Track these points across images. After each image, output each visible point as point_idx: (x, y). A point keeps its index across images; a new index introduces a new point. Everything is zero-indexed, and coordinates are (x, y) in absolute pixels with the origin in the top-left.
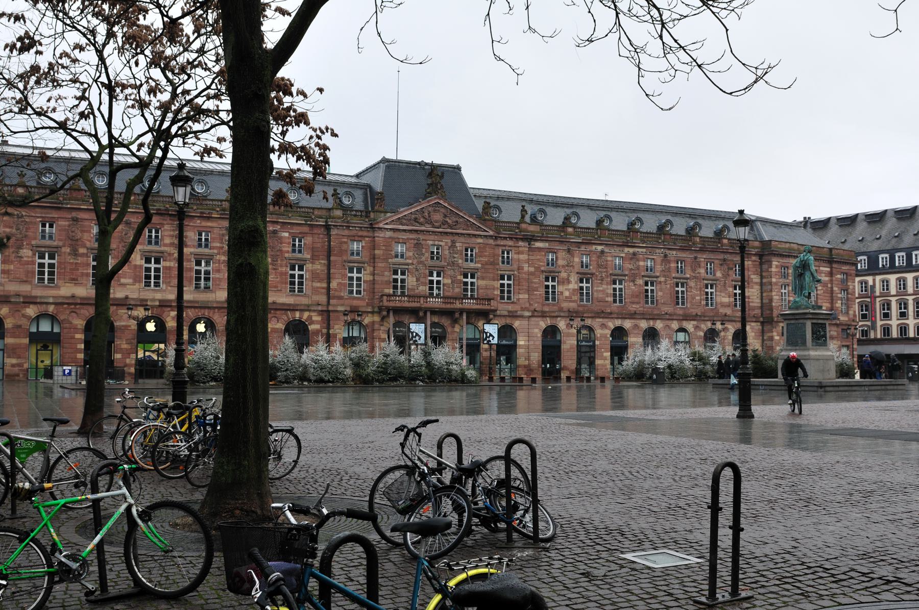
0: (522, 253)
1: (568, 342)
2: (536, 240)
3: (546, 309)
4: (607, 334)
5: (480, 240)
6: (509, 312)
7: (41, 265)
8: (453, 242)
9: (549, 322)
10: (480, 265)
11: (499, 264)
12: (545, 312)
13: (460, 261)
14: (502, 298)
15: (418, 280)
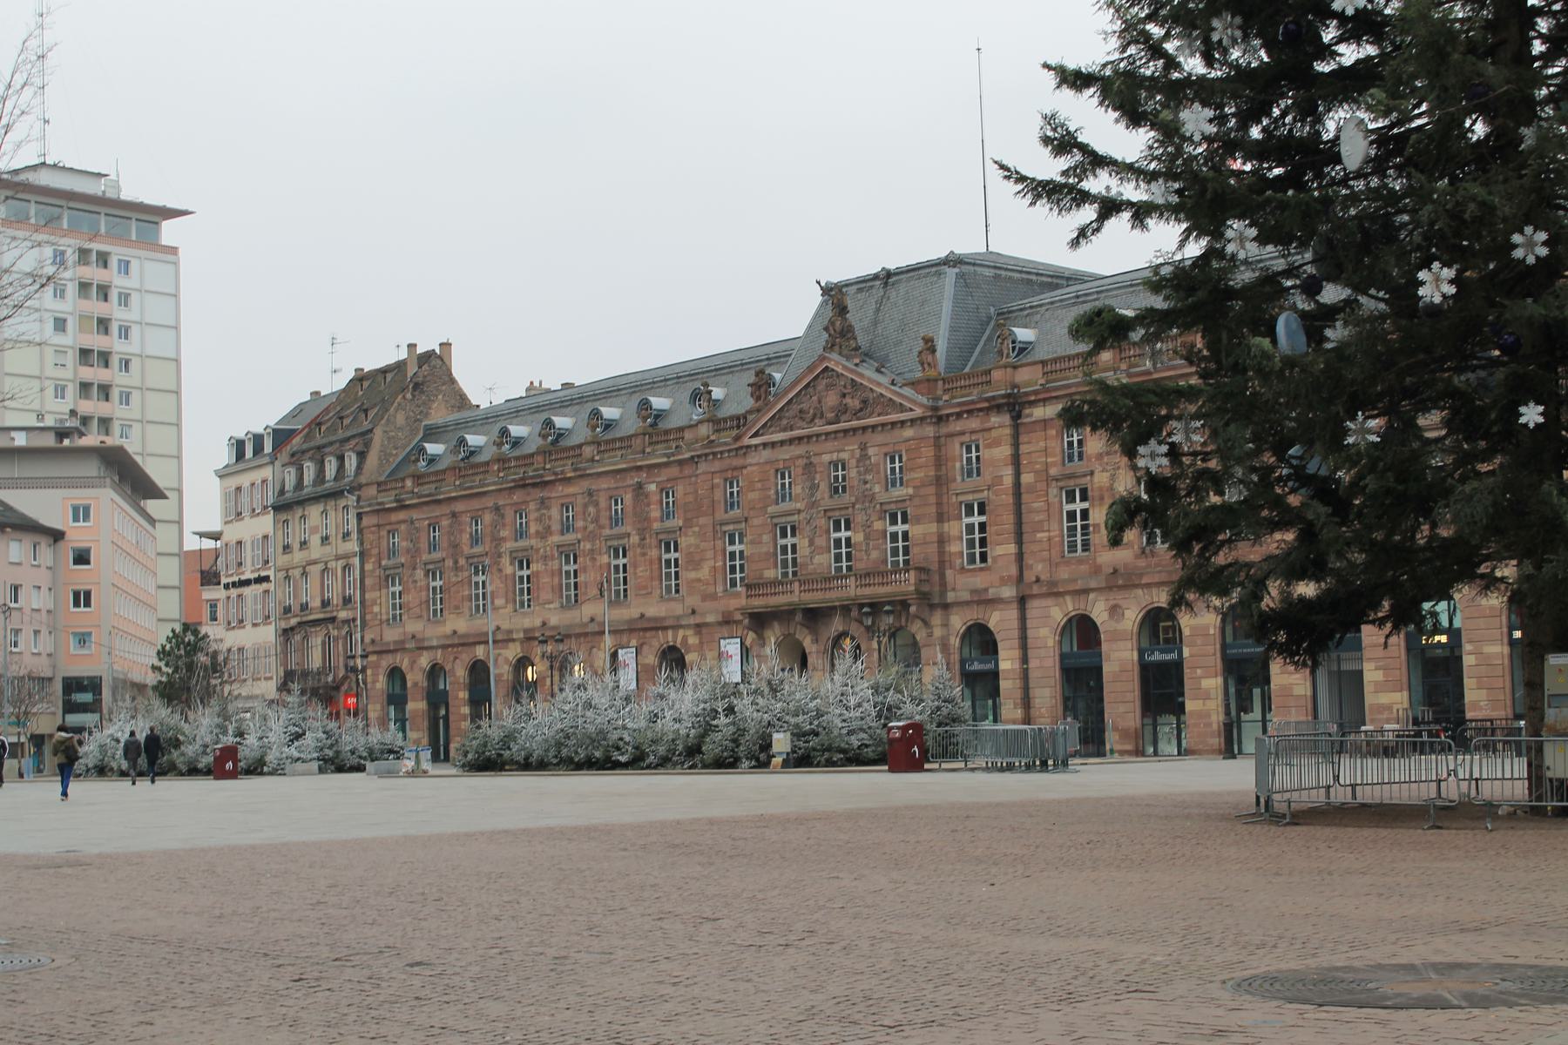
0: (996, 443)
1: (1114, 655)
2: (1032, 403)
3: (1064, 573)
4: (1207, 627)
5: (909, 433)
6: (974, 592)
8: (863, 447)
9: (1070, 606)
10: (911, 491)
11: (955, 480)
12: (1053, 584)
13: (877, 488)
14: (972, 560)
15: (811, 543)
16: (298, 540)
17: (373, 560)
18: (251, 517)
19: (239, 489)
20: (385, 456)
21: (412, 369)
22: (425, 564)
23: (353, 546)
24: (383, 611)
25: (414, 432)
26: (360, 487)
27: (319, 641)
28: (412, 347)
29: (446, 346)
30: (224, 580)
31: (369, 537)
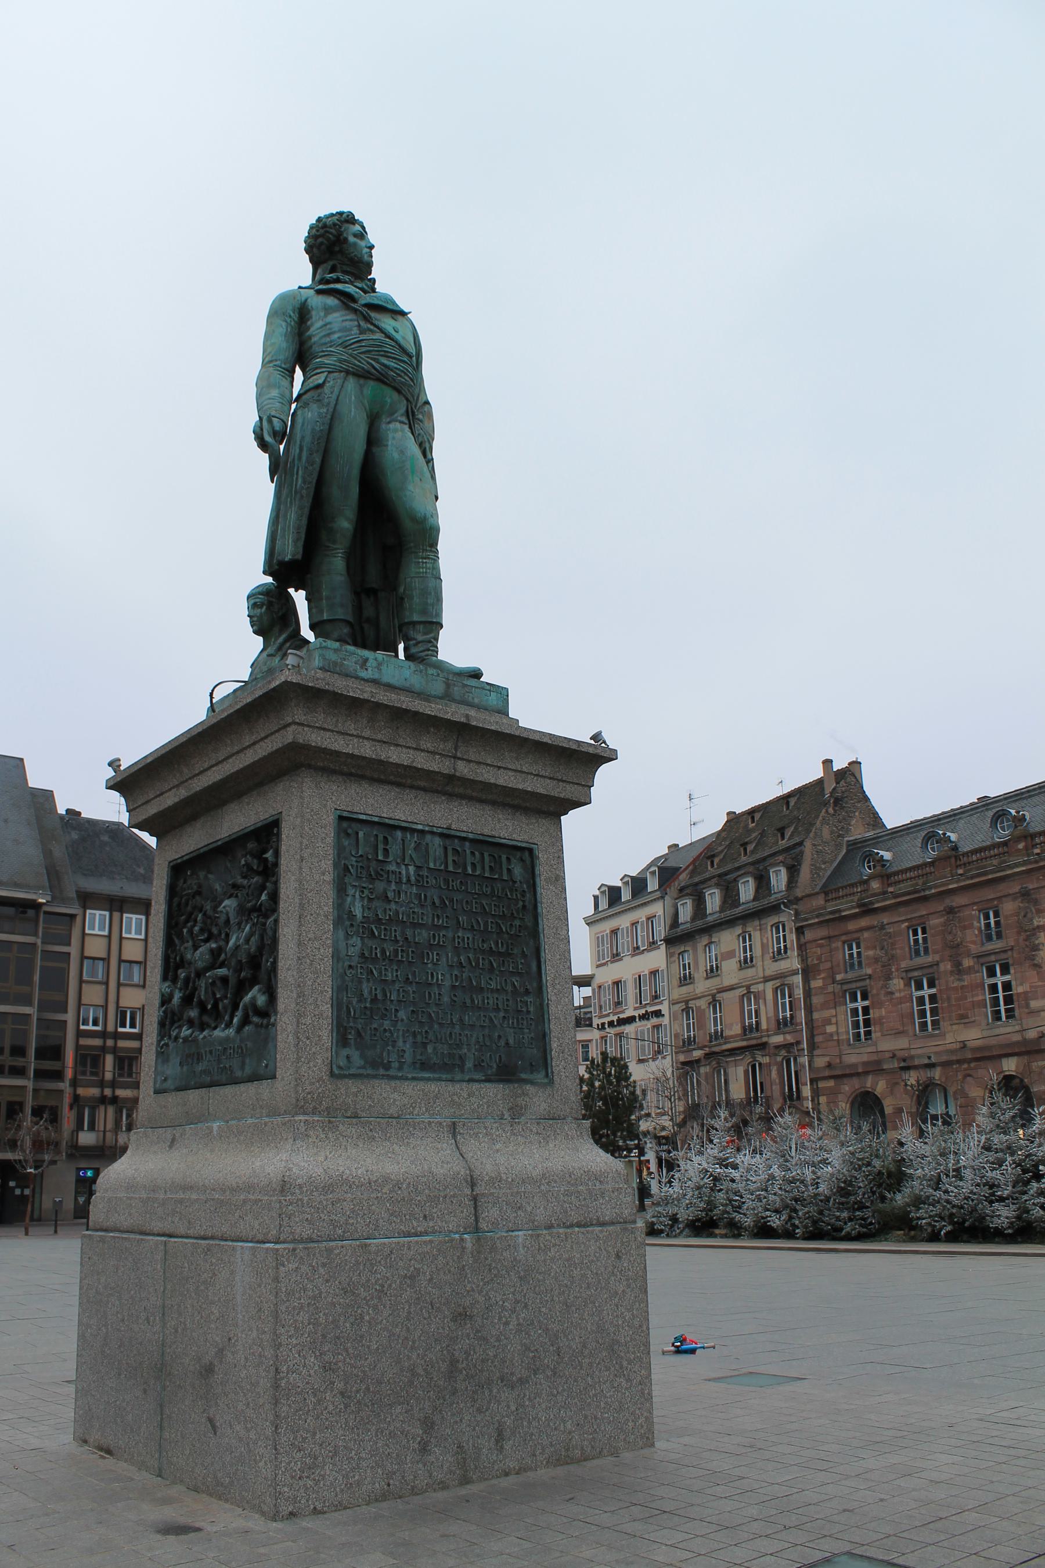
7: (921, 1001)
16: (702, 969)
17: (823, 975)
18: (633, 956)
19: (614, 932)
20: (816, 870)
21: (829, 788)
22: (906, 971)
23: (793, 962)
24: (842, 1030)
25: (838, 846)
26: (798, 900)
27: (741, 1070)
28: (827, 763)
29: (856, 764)
30: (596, 1022)
31: (815, 951)
